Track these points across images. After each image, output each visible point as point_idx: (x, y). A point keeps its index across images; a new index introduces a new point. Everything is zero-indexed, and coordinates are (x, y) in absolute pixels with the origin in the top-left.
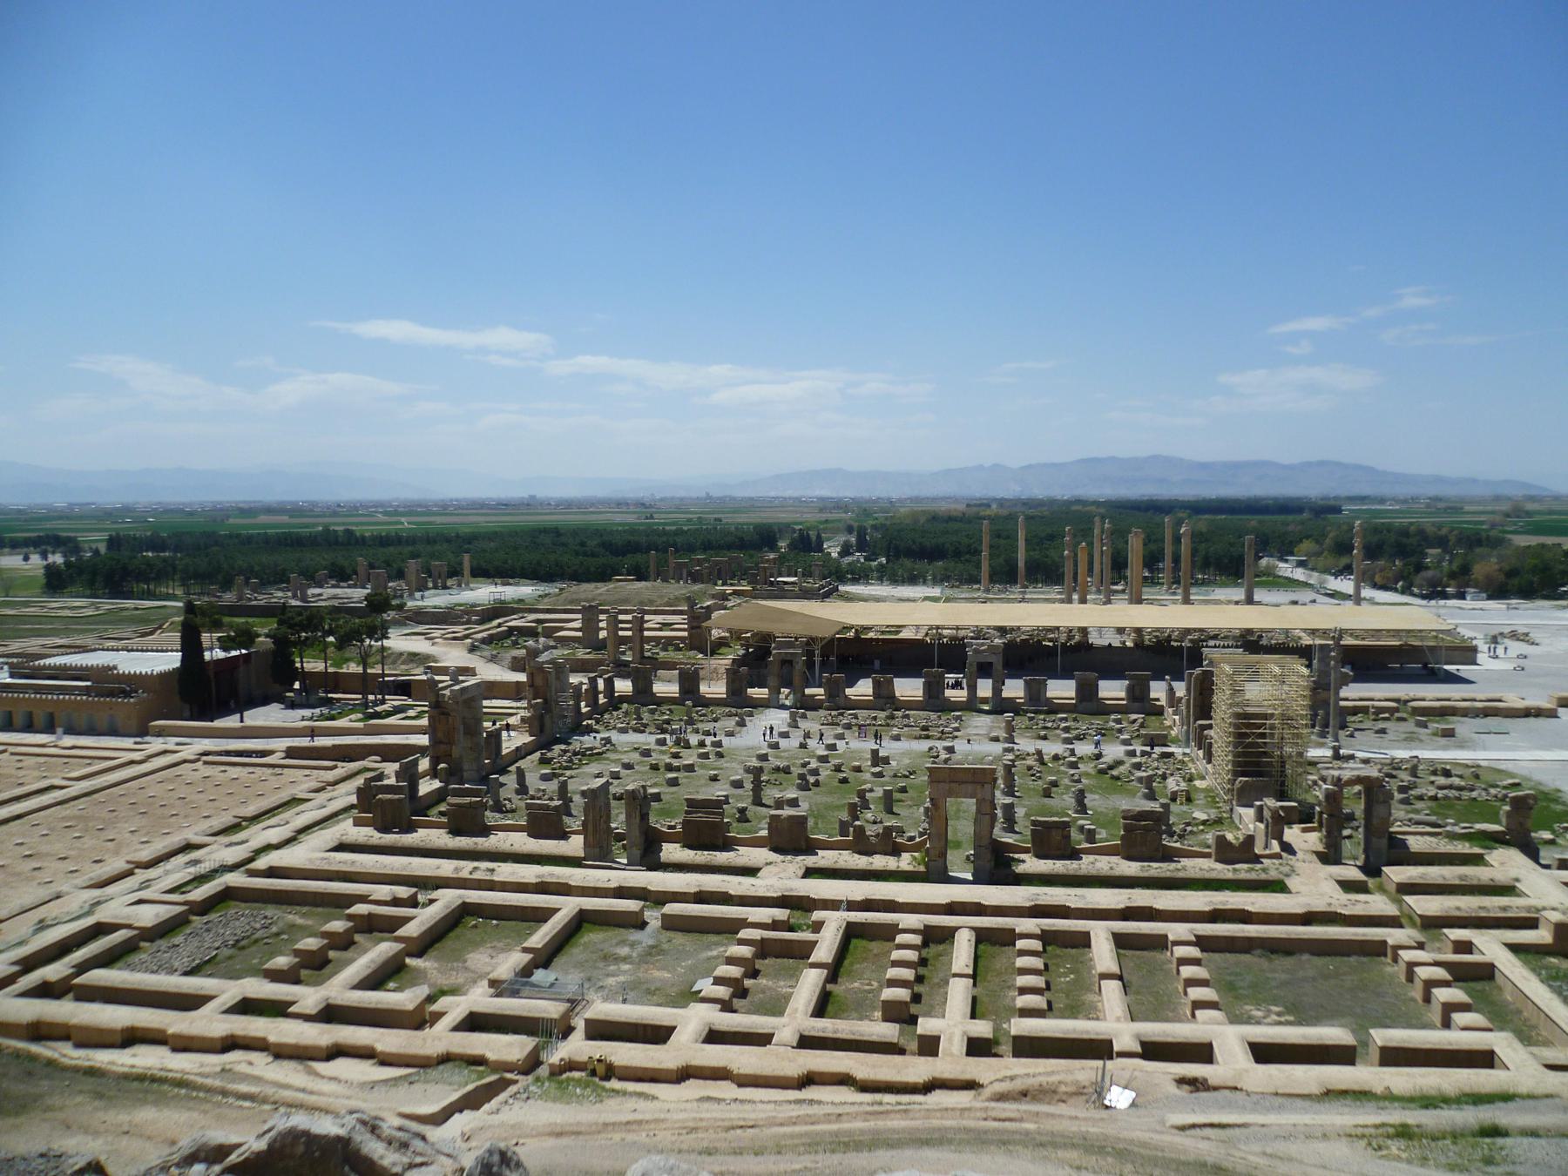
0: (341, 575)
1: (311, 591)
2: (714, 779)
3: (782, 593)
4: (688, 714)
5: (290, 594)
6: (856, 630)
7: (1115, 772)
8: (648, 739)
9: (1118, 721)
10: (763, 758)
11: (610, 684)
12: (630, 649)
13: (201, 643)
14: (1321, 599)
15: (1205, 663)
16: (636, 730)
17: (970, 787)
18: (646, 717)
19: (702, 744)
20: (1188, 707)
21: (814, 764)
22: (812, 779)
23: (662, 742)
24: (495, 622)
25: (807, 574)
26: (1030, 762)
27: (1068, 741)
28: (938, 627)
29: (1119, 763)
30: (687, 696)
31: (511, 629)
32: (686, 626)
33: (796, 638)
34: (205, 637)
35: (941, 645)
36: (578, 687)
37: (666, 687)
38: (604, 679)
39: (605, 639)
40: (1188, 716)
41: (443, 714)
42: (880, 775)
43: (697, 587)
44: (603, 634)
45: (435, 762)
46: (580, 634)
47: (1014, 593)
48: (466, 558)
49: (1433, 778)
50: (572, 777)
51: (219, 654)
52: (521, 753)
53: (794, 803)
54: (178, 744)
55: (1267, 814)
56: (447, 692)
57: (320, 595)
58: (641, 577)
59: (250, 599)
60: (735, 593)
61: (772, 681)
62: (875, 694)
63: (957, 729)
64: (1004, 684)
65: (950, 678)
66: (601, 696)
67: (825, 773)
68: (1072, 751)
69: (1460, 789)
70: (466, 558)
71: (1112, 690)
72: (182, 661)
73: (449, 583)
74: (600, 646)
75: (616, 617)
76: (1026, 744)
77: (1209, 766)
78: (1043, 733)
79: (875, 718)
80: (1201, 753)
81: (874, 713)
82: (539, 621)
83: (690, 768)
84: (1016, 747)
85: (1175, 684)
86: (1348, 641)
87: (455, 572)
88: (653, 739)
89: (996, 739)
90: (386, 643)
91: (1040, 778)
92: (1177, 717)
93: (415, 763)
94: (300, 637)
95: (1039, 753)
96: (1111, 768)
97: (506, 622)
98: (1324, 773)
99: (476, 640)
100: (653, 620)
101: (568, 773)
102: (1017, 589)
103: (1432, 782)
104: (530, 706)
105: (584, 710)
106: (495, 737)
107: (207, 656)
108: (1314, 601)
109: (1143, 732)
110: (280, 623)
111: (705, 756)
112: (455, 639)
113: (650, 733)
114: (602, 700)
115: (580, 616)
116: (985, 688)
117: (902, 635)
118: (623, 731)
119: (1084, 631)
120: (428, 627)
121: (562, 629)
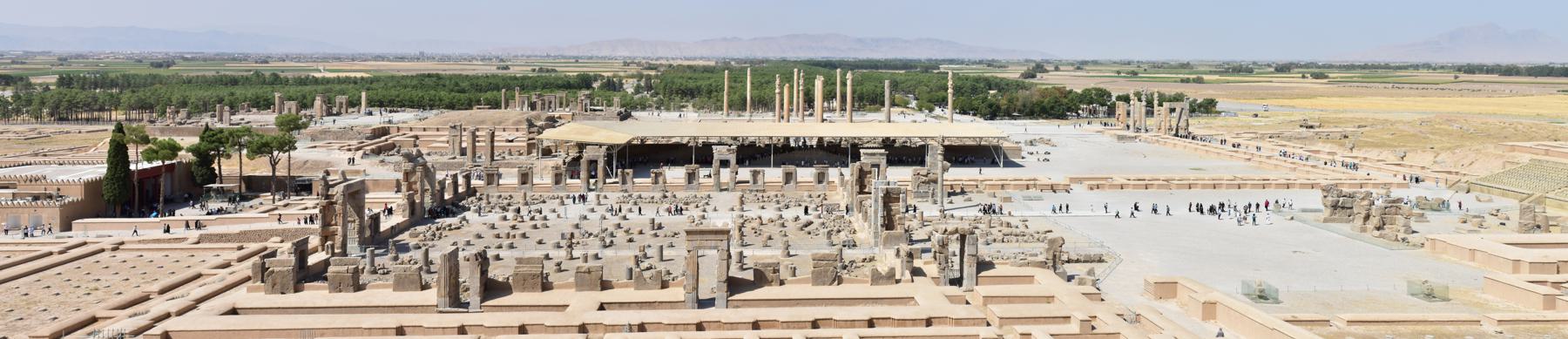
0: (264, 104)
1: (236, 118)
2: (540, 242)
5: (216, 119)
6: (642, 140)
7: (807, 229)
8: (494, 217)
9: (810, 196)
10: (577, 226)
11: (468, 178)
13: (128, 157)
14: (929, 119)
15: (862, 158)
17: (713, 243)
18: (493, 200)
20: (852, 187)
21: (611, 229)
22: (608, 241)
23: (505, 218)
24: (383, 138)
25: (610, 104)
26: (755, 224)
27: (779, 209)
28: (695, 138)
29: (810, 223)
33: (601, 146)
34: (132, 151)
35: (697, 147)
36: (442, 183)
37: (510, 178)
38: (464, 177)
40: (852, 193)
42: (656, 235)
44: (464, 145)
45: (326, 236)
46: (447, 145)
48: (364, 94)
49: (1000, 228)
50: (433, 246)
51: (146, 165)
52: (396, 230)
53: (596, 257)
54: (98, 237)
55: (902, 253)
57: (243, 119)
58: (495, 105)
59: (180, 124)
61: (583, 174)
63: (707, 204)
64: (737, 173)
65: (703, 172)
67: (620, 234)
68: (781, 217)
69: (1016, 235)
70: (364, 94)
71: (806, 174)
72: (108, 169)
73: (350, 110)
74: (463, 152)
76: (753, 211)
77: (866, 224)
78: (762, 204)
79: (653, 198)
80: (861, 215)
82: (417, 137)
83: (524, 236)
84: (745, 214)
85: (844, 170)
86: (946, 143)
87: (354, 104)
89: (733, 210)
90: (292, 153)
91: (760, 234)
92: (845, 193)
93: (306, 241)
94: (219, 151)
95: (760, 218)
96: (806, 226)
98: (937, 226)
100: (501, 136)
101: (430, 243)
102: (747, 114)
103: (1000, 231)
105: (447, 197)
106: (375, 219)
107: (132, 167)
108: (926, 121)
109: (825, 202)
110: (202, 139)
111: (535, 227)
114: (461, 190)
115: (447, 133)
116: (725, 174)
119: (787, 139)
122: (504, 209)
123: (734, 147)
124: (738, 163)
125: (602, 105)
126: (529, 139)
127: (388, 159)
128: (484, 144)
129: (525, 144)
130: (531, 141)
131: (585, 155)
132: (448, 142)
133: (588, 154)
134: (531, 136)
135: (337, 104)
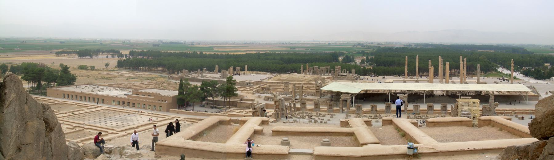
3: (342, 78)
4: (317, 114)
11: (294, 104)
12: (298, 95)
16: (302, 118)
19: (321, 122)
28: (390, 90)
30: (316, 109)
31: (263, 89)
32: (315, 89)
33: (348, 93)
37: (310, 106)
38: (293, 104)
39: (291, 92)
41: (256, 111)
43: (316, 76)
47: (414, 78)
48: (246, 66)
56: (257, 106)
58: (299, 72)
60: (328, 78)
61: (341, 106)
62: (372, 110)
64: (408, 106)
66: (292, 108)
70: (246, 66)
75: (295, 86)
79: (371, 116)
81: (371, 115)
82: (270, 86)
88: (308, 121)
97: (261, 86)
99: (254, 91)
104: (275, 111)
112: (247, 91)
113: (307, 119)
117: (379, 92)
118: (299, 118)
119: (432, 91)
120: (238, 87)
121: (278, 88)
122: (310, 118)
123: (407, 95)
124: (409, 102)
125: (346, 73)
126: (317, 89)
127: (262, 95)
128: (299, 90)
129: (315, 91)
130: (317, 90)
131: (342, 97)
132: (283, 89)
133: (342, 97)
134: (318, 88)
135: (236, 70)
